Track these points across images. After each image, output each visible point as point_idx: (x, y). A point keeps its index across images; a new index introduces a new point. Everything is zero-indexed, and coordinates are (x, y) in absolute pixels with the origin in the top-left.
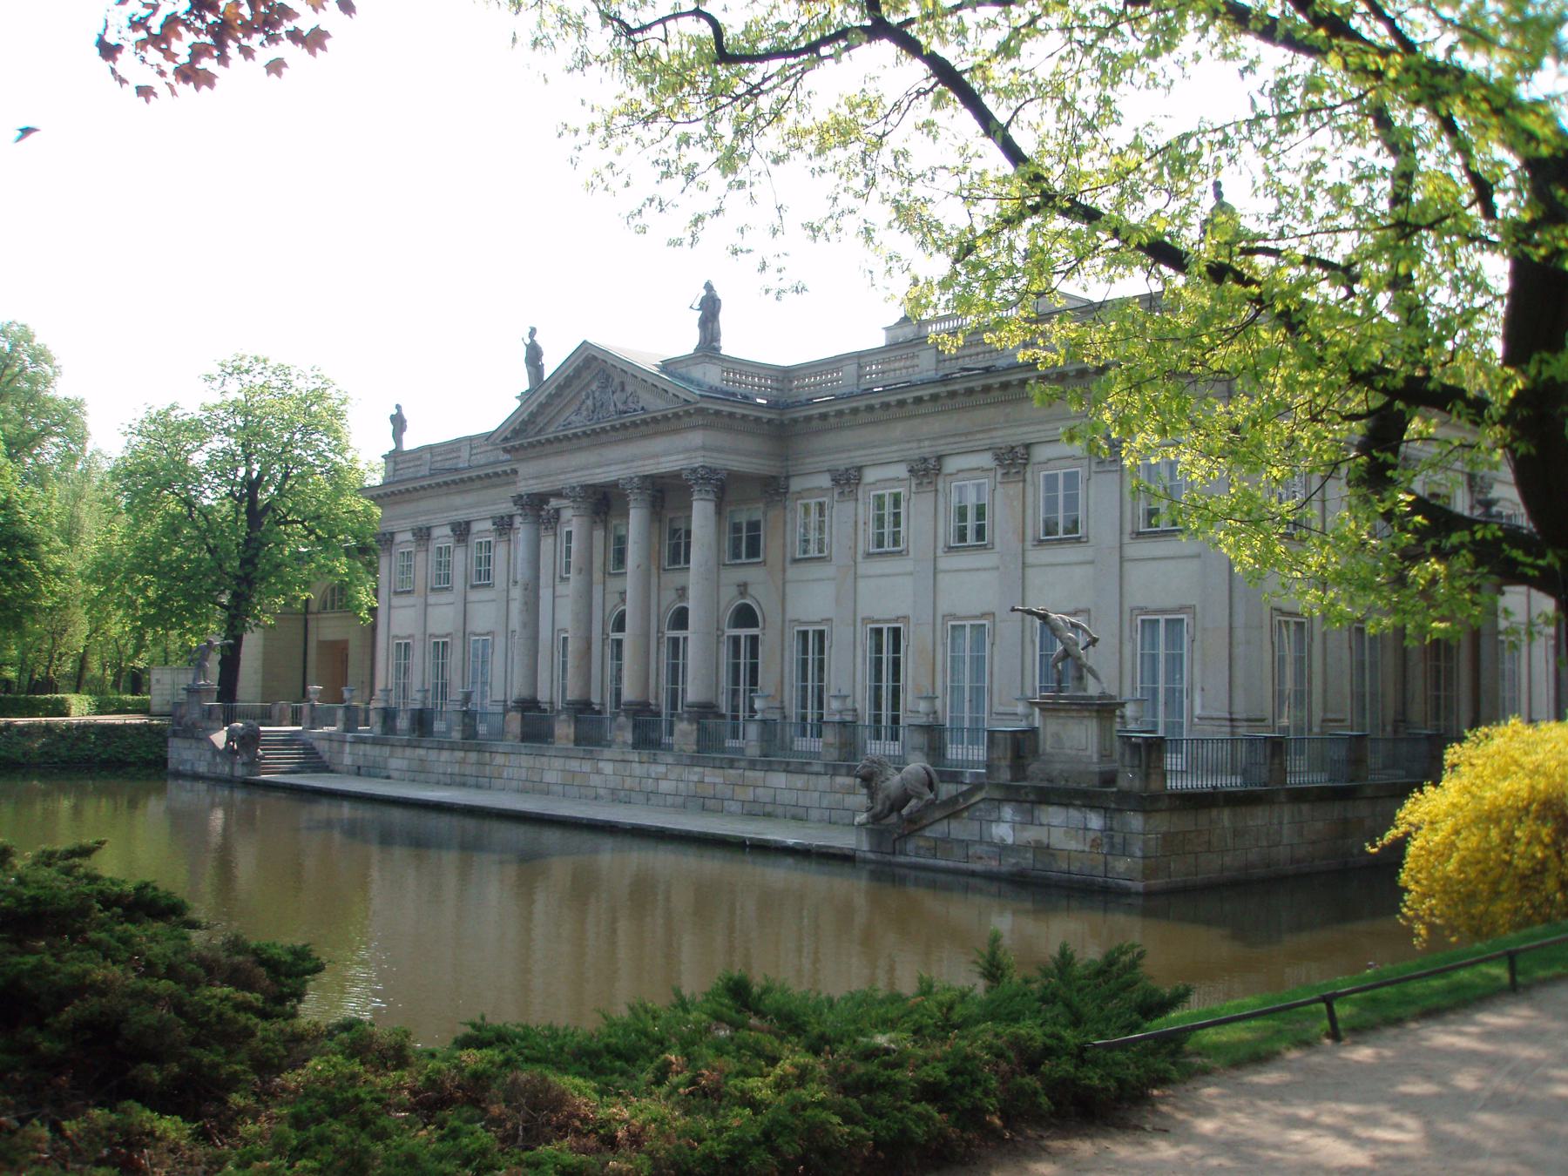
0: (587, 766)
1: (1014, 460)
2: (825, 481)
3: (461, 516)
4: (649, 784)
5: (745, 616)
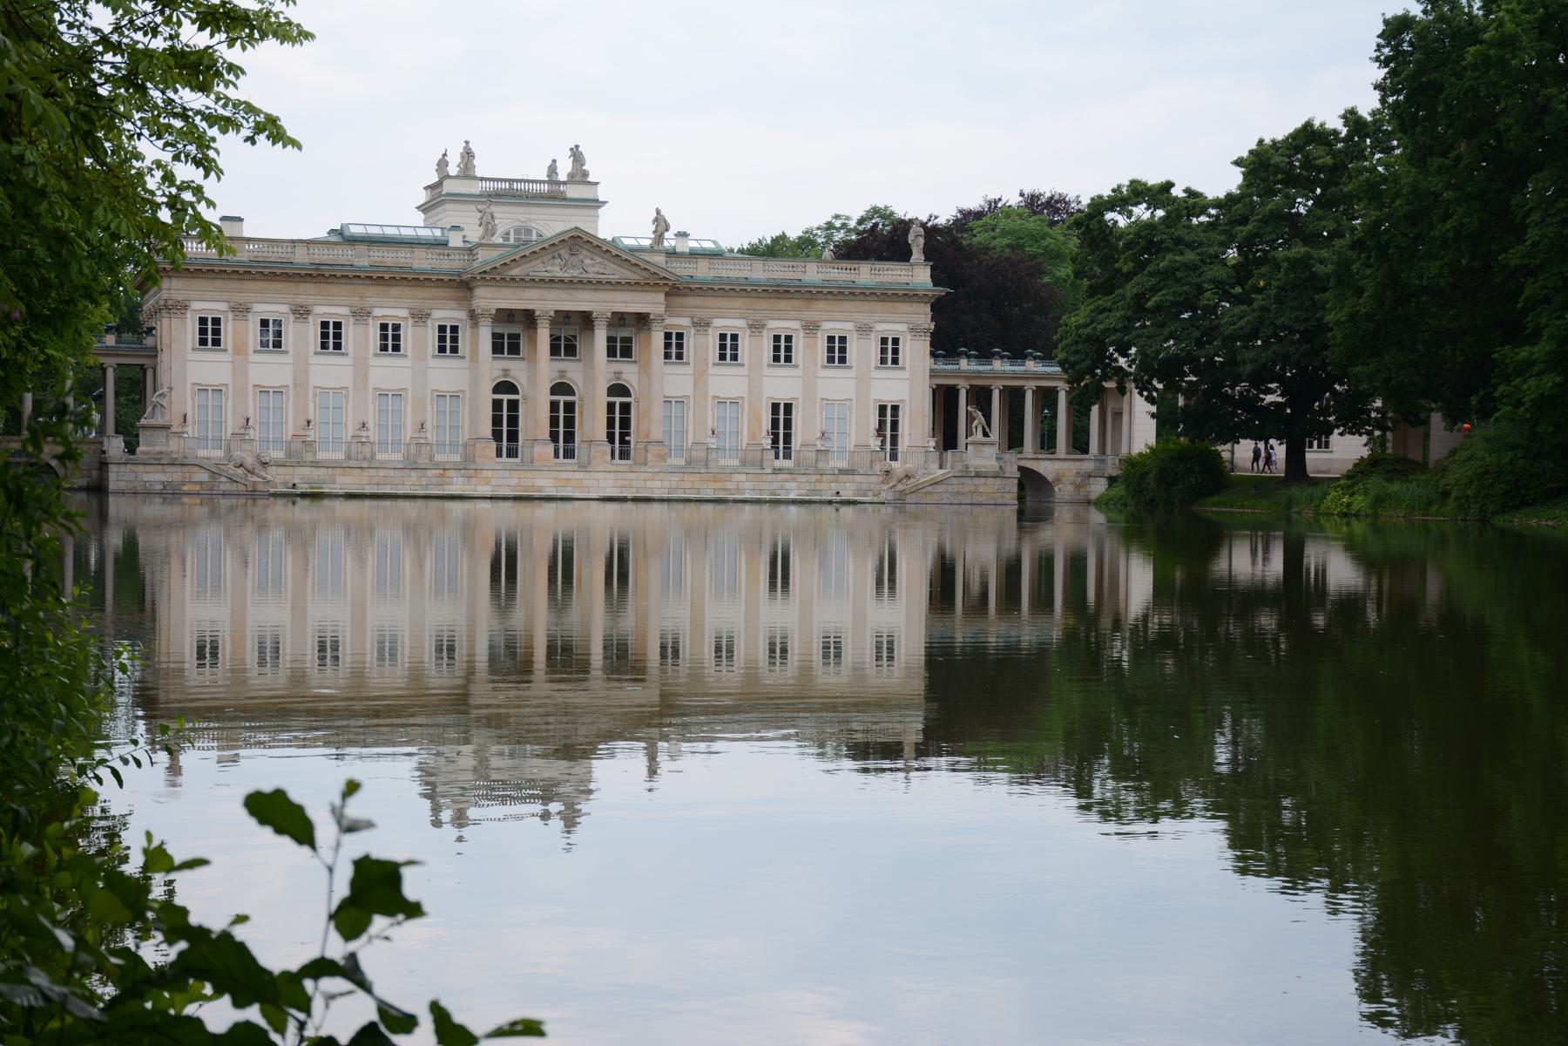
0: (578, 475)
1: (811, 328)
2: (685, 322)
3: (301, 300)
4: (641, 484)
5: (618, 390)
